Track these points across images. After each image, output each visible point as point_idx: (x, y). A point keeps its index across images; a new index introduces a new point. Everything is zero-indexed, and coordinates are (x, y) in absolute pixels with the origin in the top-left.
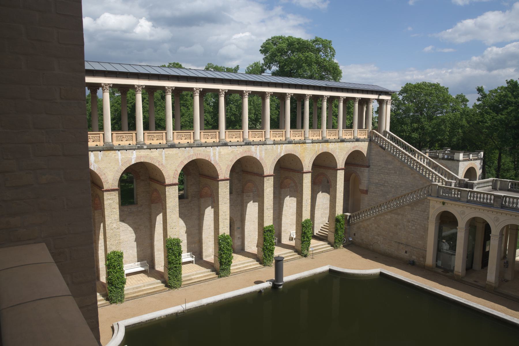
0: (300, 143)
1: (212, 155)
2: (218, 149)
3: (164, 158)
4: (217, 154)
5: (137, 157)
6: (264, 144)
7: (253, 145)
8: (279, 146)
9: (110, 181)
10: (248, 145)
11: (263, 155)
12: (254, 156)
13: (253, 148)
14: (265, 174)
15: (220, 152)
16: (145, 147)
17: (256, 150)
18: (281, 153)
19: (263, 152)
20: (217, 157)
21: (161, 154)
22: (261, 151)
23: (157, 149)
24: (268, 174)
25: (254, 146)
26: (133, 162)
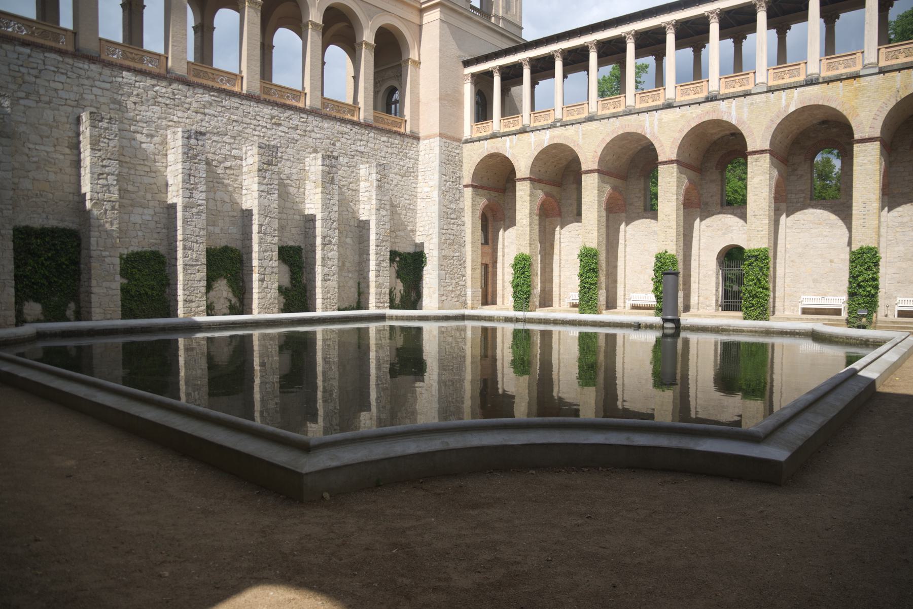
0: (841, 80)
1: (647, 124)
2: (656, 115)
3: (581, 136)
4: (656, 123)
5: (552, 138)
6: (746, 94)
7: (723, 99)
8: (783, 94)
9: (523, 169)
10: (712, 100)
11: (745, 116)
12: (725, 118)
13: (723, 105)
14: (750, 148)
15: (660, 120)
16: (558, 124)
17: (730, 107)
18: (788, 106)
19: (746, 109)
20: (656, 127)
21: (577, 132)
22: (739, 108)
23: (572, 124)
24: (758, 148)
25: (726, 101)
26: (546, 145)
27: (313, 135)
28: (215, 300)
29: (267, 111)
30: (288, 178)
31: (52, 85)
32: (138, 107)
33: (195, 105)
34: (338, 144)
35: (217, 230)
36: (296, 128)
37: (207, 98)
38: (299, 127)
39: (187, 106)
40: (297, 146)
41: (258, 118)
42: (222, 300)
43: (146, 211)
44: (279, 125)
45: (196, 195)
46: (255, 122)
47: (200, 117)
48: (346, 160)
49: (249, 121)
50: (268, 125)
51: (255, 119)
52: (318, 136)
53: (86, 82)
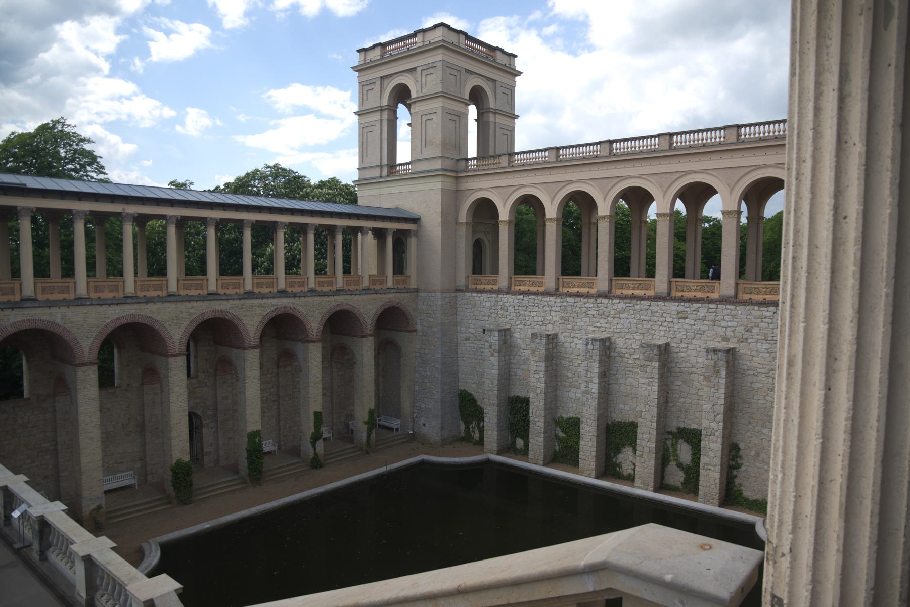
27: (724, 324)
28: (623, 461)
29: (673, 307)
30: (693, 366)
31: (532, 314)
32: (576, 320)
33: (613, 312)
34: (755, 330)
35: (627, 408)
36: (704, 319)
37: (622, 305)
38: (707, 318)
39: (607, 314)
40: (705, 337)
41: (665, 315)
42: (628, 462)
43: (578, 391)
44: (685, 318)
45: (591, 385)
46: (661, 319)
47: (616, 321)
48: (766, 346)
49: (656, 319)
50: (675, 321)
51: (662, 316)
52: (730, 324)
53: (547, 309)
